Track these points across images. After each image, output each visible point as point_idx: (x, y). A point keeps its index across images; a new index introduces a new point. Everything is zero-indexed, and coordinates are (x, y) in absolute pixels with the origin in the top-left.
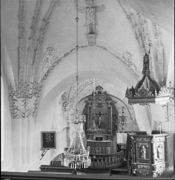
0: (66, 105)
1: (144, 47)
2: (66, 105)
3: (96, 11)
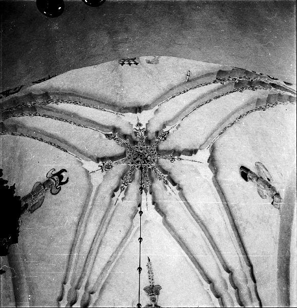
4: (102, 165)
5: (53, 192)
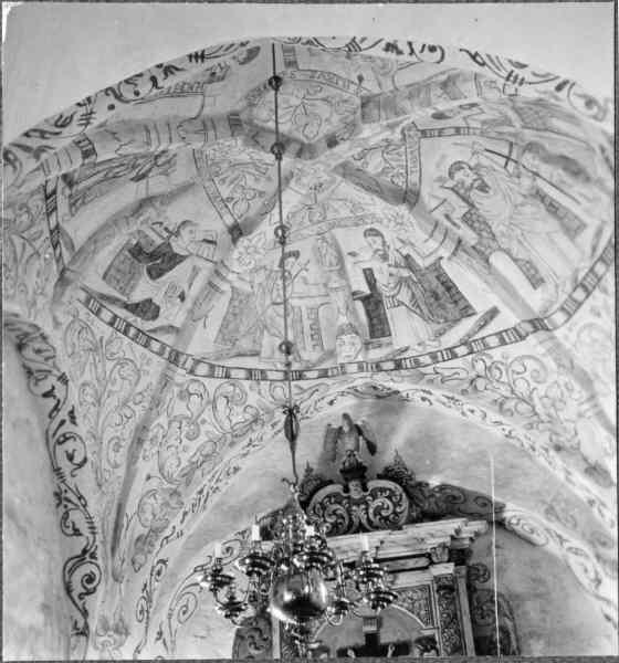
0: (90, 579)
2: (90, 579)
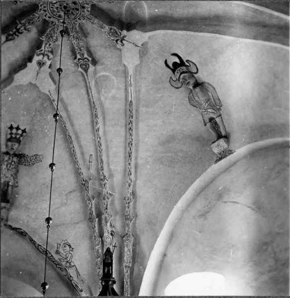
1: (101, 236)
3: (20, 163)
4: (119, 42)
5: (196, 72)
